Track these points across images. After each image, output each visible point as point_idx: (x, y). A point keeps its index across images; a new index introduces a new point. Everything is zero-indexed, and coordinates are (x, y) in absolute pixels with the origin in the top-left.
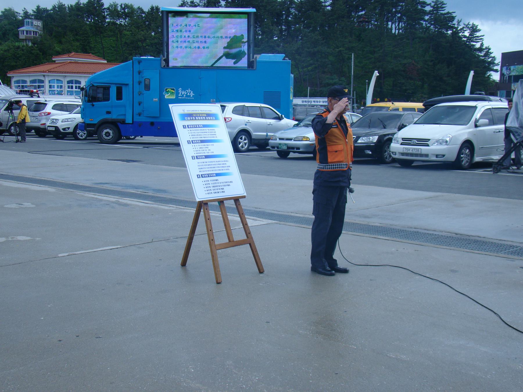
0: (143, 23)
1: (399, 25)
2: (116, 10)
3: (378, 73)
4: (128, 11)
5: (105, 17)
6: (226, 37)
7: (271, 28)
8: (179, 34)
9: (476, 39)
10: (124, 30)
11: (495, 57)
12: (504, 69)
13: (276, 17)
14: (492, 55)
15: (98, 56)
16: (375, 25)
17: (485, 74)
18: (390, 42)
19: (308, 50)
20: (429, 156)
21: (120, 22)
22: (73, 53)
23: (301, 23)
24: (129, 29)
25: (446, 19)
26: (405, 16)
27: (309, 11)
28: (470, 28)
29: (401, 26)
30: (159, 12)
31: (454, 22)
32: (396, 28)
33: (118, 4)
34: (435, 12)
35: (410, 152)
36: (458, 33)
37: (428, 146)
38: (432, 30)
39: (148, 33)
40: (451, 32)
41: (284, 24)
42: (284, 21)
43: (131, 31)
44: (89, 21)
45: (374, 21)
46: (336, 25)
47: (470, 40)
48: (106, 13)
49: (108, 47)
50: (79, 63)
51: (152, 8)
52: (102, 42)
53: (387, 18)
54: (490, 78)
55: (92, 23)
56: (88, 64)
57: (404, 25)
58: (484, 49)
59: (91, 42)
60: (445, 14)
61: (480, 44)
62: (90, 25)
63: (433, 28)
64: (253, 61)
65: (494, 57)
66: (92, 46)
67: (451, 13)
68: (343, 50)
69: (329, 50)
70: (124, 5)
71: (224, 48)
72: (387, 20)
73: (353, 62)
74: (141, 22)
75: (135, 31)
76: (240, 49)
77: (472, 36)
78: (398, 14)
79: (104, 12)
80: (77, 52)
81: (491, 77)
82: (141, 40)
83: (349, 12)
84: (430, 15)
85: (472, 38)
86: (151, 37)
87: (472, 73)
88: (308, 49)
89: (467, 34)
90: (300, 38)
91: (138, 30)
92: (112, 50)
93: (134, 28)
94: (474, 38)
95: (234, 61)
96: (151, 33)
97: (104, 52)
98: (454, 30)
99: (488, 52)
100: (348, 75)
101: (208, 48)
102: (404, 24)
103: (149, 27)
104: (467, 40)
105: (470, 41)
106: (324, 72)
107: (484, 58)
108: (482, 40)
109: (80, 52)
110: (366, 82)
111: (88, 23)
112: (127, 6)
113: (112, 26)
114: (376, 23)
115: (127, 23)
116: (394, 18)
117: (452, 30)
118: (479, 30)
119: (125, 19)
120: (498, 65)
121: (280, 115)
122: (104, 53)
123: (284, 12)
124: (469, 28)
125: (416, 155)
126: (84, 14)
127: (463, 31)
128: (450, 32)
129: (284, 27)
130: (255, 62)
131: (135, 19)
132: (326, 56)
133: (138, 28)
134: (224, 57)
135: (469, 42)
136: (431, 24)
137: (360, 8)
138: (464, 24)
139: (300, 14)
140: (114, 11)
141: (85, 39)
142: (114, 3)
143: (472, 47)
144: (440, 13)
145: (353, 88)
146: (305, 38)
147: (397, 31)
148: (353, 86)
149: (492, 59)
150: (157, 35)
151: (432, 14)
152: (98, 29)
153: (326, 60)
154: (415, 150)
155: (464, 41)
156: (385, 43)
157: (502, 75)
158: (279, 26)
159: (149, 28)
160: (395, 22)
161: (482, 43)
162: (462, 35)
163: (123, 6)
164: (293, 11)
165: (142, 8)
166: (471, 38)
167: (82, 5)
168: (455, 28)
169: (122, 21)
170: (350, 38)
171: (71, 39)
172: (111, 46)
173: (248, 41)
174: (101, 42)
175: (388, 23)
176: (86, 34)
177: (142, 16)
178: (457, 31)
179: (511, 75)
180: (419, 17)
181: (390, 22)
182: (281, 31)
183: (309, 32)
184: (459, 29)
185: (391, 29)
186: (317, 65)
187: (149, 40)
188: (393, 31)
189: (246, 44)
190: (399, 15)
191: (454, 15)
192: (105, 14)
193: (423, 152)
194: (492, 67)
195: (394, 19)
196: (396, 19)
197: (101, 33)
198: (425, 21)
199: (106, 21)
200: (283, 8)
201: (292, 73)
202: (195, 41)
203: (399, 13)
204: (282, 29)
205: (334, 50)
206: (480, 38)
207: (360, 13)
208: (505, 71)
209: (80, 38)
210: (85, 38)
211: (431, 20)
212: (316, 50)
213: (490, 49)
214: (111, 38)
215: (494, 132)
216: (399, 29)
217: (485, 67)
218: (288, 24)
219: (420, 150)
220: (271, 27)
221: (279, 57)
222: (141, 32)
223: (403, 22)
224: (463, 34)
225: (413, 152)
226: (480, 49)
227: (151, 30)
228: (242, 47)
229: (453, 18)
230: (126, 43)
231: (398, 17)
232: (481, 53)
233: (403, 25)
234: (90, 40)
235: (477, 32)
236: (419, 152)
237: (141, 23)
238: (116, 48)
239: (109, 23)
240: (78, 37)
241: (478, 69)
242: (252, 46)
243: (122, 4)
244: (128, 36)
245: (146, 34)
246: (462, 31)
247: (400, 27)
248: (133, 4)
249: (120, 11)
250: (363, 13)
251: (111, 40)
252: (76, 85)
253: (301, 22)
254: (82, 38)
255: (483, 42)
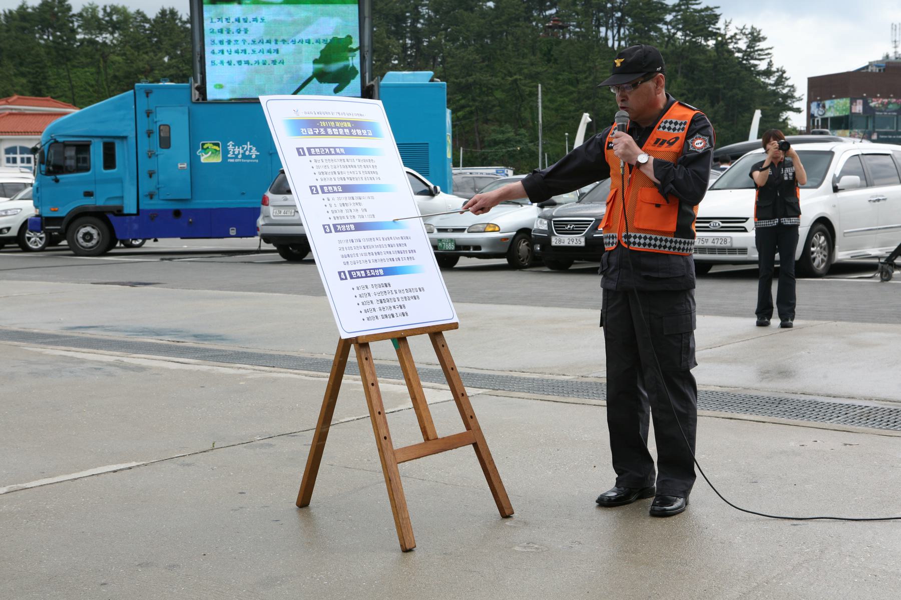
0: (146, 39)
1: (619, 32)
2: (94, 16)
3: (590, 117)
4: (117, 18)
5: (73, 31)
6: (318, 41)
7: (387, 43)
8: (224, 37)
9: (759, 55)
10: (111, 53)
11: (795, 86)
12: (814, 105)
13: (395, 24)
14: (788, 83)
15: (64, 102)
16: (575, 33)
17: (779, 117)
18: (605, 62)
19: (455, 80)
20: (748, 251)
21: (104, 39)
22: (15, 97)
23: (441, 32)
24: (120, 51)
25: (703, 19)
26: (629, 16)
27: (454, 10)
28: (748, 34)
29: (624, 34)
30: (176, 19)
31: (718, 25)
32: (614, 37)
33: (97, 7)
34: (683, 7)
35: (709, 244)
36: (727, 44)
37: (745, 231)
38: (678, 39)
39: (158, 57)
40: (714, 42)
41: (409, 35)
42: (408, 30)
43: (124, 54)
44: (47, 38)
45: (573, 26)
46: (505, 34)
47: (749, 55)
48: (76, 24)
49: (82, 86)
50: (26, 114)
51: (163, 13)
52: (69, 76)
53: (598, 20)
54: (787, 124)
55: (51, 41)
56: (44, 117)
57: (630, 32)
58: (774, 72)
59: (49, 76)
60: (702, 10)
61: (767, 64)
62: (46, 46)
63: (682, 36)
64: (373, 86)
65: (792, 86)
66: (52, 83)
67: (711, 9)
68: (520, 79)
69: (494, 79)
70: (110, 7)
71: (315, 61)
72: (597, 23)
73: (540, 100)
74: (142, 37)
75: (133, 54)
76: (345, 63)
77: (752, 50)
78: (617, 11)
79: (72, 22)
80: (23, 95)
81: (789, 122)
82: (143, 70)
83: (529, 10)
84: (674, 14)
85: (751, 52)
86: (162, 65)
87: (758, 114)
88: (457, 79)
89: (743, 44)
90: (439, 60)
91: (138, 52)
92: (89, 91)
93: (129, 48)
94: (756, 53)
95: (335, 85)
96: (161, 58)
97: (73, 94)
98: (720, 39)
99: (781, 77)
100: (531, 124)
101: (282, 62)
102: (628, 30)
103: (158, 48)
104: (744, 56)
105: (749, 58)
106: (486, 121)
107: (774, 88)
108: (769, 56)
109: (29, 96)
110: (565, 136)
111: (42, 42)
112: (115, 10)
113: (88, 46)
114: (578, 30)
115: (117, 40)
116: (609, 20)
117: (716, 39)
118: (764, 39)
119: (112, 33)
120: (800, 99)
121: (432, 186)
122: (75, 98)
123: (408, 14)
124: (746, 35)
125: (722, 250)
126: (35, 26)
127: (736, 39)
128: (711, 43)
129: (408, 41)
130: (376, 88)
131: (131, 32)
132: (490, 91)
133: (137, 48)
134: (315, 80)
135: (747, 60)
136: (678, 29)
137: (548, 4)
138: (737, 28)
139: (438, 17)
140: (91, 20)
141: (37, 71)
142: (90, 4)
143: (753, 69)
144: (693, 9)
145: (542, 147)
146: (449, 59)
147: (616, 44)
148: (543, 144)
149: (790, 90)
150: (174, 61)
151: (678, 11)
152: (61, 52)
153: (490, 98)
154: (720, 241)
155: (738, 58)
156: (597, 64)
157: (811, 117)
158: (399, 40)
159: (159, 48)
160: (613, 27)
161: (771, 61)
162: (734, 48)
163: (108, 10)
164: (424, 11)
165: (145, 13)
166: (749, 54)
167: (30, 10)
168: (721, 35)
169: (105, 38)
170: (532, 57)
171: (12, 73)
172: (88, 83)
173: (361, 48)
174: (67, 77)
175: (599, 29)
176: (38, 62)
177: (144, 27)
178: (724, 41)
179: (826, 116)
180: (655, 17)
181: (603, 26)
182: (404, 47)
183: (457, 48)
184: (727, 37)
185: (606, 39)
186: (473, 108)
187: (159, 70)
188: (610, 43)
189: (358, 53)
190: (619, 14)
191: (717, 12)
192: (74, 26)
193: (737, 244)
194: (790, 103)
195: (611, 21)
196: (613, 21)
197: (69, 60)
198: (666, 23)
199: (75, 38)
200: (407, 7)
201: (448, 108)
202: (257, 51)
203: (620, 10)
204: (405, 44)
205: (503, 79)
206: (766, 52)
207: (548, 13)
208: (815, 110)
209: (27, 70)
210: (38, 69)
211: (676, 21)
212: (470, 80)
213: (784, 72)
214: (87, 69)
215: (870, 201)
216: (619, 40)
217: (778, 104)
218: (417, 35)
219: (729, 240)
220: (387, 41)
221: (423, 77)
222: (145, 56)
223: (626, 27)
224: (735, 46)
225: (715, 244)
226: (768, 73)
227: (161, 52)
228: (350, 58)
229: (716, 18)
230: (115, 77)
231: (618, 18)
232: (769, 79)
233: (627, 32)
234: (48, 72)
235: (759, 41)
236: (728, 245)
237: (144, 38)
238: (96, 87)
239: (82, 41)
240: (23, 69)
241: (765, 107)
242: (367, 57)
243: (105, 7)
244: (119, 63)
245: (153, 59)
246: (734, 41)
247: (621, 35)
248: (126, 5)
249: (103, 19)
250: (553, 11)
251: (86, 72)
252: (22, 156)
253: (442, 30)
254: (31, 71)
255: (772, 59)
